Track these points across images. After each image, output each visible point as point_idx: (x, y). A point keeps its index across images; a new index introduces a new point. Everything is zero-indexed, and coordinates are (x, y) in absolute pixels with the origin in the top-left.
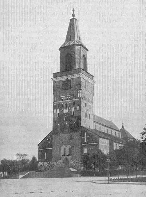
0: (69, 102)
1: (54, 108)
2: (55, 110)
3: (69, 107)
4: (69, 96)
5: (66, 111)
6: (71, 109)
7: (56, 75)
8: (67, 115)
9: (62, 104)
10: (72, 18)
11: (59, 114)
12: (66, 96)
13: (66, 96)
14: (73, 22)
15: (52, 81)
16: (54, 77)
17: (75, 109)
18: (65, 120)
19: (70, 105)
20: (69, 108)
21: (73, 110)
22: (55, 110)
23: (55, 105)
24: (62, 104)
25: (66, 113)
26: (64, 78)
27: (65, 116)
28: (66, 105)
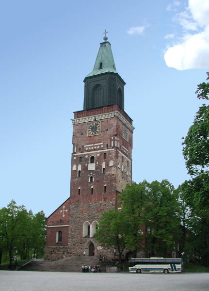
0: (97, 154)
1: (74, 162)
2: (75, 166)
3: (97, 161)
4: (97, 146)
5: (92, 167)
6: (100, 163)
7: (78, 114)
8: (93, 173)
9: (87, 157)
10: (104, 41)
11: (80, 171)
12: (93, 145)
13: (93, 145)
14: (105, 44)
15: (71, 124)
16: (75, 118)
17: (107, 164)
19: (98, 158)
20: (97, 164)
21: (104, 166)
22: (75, 166)
23: (75, 158)
24: (87, 157)
25: (92, 171)
26: (91, 119)
27: (91, 175)
28: (93, 158)
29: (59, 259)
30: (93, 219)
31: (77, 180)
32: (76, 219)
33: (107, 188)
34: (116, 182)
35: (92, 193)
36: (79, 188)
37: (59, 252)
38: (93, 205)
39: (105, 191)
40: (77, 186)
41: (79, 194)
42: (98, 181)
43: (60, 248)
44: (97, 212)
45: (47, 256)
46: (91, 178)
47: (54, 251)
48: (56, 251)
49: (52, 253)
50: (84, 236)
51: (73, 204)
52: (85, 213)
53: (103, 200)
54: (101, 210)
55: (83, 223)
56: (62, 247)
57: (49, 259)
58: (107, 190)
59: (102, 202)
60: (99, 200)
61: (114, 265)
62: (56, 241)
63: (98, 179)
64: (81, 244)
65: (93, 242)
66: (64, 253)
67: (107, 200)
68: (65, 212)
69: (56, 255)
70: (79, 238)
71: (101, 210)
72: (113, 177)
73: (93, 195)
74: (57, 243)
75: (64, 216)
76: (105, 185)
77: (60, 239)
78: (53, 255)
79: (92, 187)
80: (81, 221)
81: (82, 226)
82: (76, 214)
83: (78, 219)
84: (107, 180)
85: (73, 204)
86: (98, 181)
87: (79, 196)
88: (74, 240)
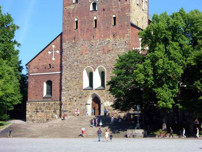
18: (91, 8)
29: (47, 120)
30: (98, 63)
31: (72, 7)
32: (73, 63)
33: (117, 20)
34: (129, 11)
35: (96, 26)
36: (76, 20)
37: (48, 111)
38: (97, 42)
39: (115, 24)
40: (74, 16)
41: (77, 28)
42: (104, 10)
43: (49, 104)
44: (103, 54)
45: (31, 116)
46: (94, 5)
47: (40, 109)
48: (43, 108)
49: (37, 112)
50: (84, 88)
51: (67, 42)
52: (86, 54)
53: (111, 36)
54: (109, 51)
55: (82, 69)
56: (52, 102)
57: (33, 120)
58: (117, 22)
59: (111, 39)
60: (105, 37)
61: (133, 127)
62: (43, 94)
63: (104, 6)
64: (80, 98)
65: (99, 96)
66: (55, 112)
67: (118, 38)
68: (55, 53)
69: (43, 114)
70: (78, 90)
71: (109, 51)
72: (126, 4)
73: (97, 29)
74: (44, 98)
75: (53, 59)
76: (114, 16)
77: (50, 92)
78: (39, 114)
79: (95, 18)
80: (80, 66)
81: (81, 74)
82: (73, 56)
83: (76, 64)
84: (118, 8)
85: (67, 42)
86: (104, 10)
87: (76, 31)
88: (70, 92)
